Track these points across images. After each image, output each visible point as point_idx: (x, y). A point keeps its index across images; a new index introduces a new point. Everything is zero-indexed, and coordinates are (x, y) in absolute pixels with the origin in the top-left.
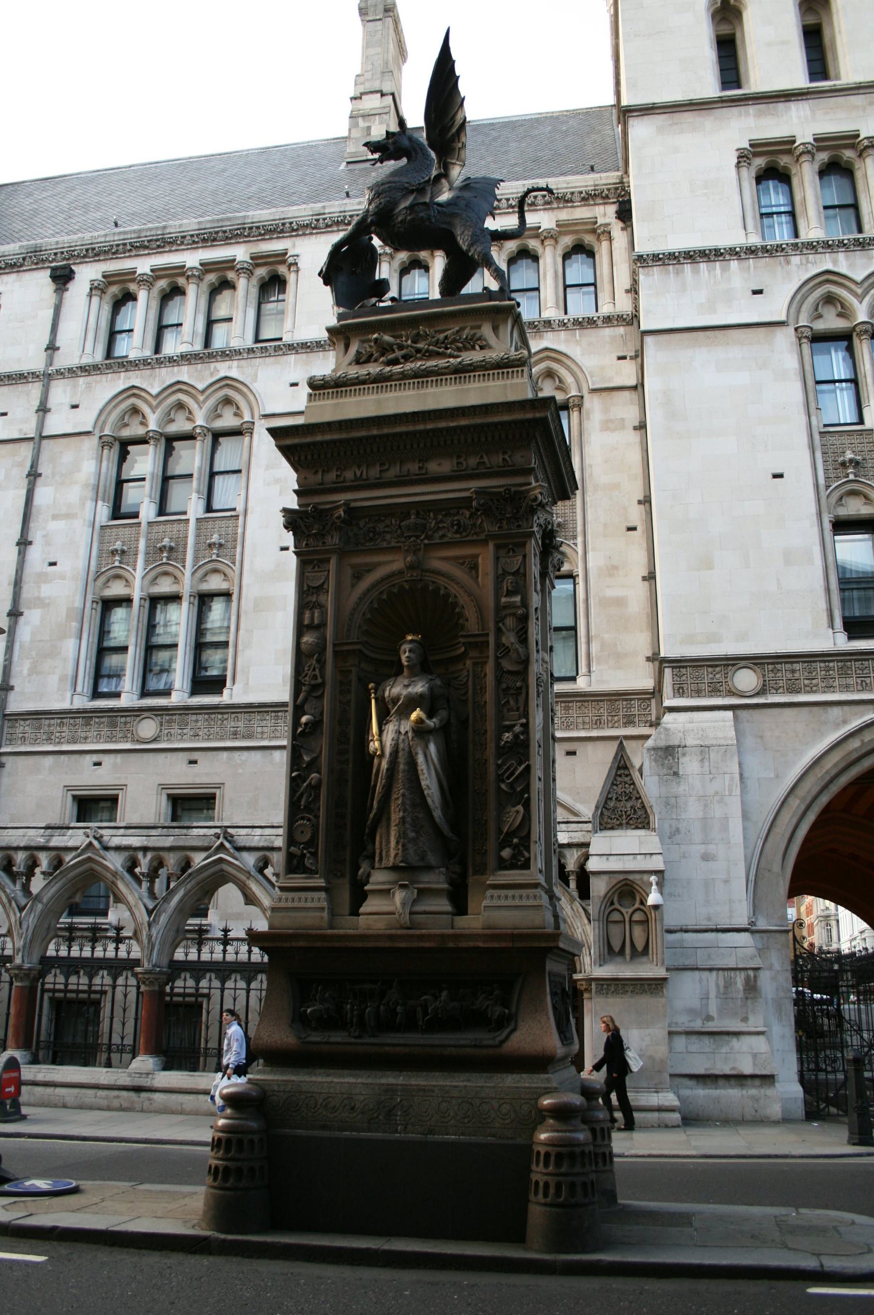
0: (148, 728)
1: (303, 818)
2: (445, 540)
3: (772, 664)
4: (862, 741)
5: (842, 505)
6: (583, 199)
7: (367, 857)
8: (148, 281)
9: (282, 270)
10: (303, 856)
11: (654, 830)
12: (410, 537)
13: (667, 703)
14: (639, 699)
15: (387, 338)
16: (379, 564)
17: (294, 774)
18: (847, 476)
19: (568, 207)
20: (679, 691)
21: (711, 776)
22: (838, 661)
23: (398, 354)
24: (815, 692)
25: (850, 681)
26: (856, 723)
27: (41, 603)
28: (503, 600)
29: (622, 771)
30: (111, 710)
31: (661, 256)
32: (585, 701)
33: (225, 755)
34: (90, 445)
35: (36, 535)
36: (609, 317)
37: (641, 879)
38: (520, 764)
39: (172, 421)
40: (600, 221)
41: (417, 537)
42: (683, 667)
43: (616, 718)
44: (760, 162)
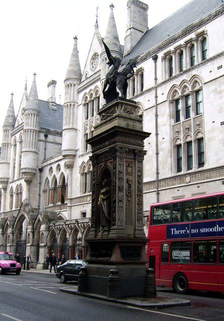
0: (188, 179)
8: (175, 52)
9: (205, 36)
15: (104, 114)
27: (162, 150)
30: (179, 176)
33: (205, 184)
34: (167, 104)
35: (159, 132)
39: (185, 91)
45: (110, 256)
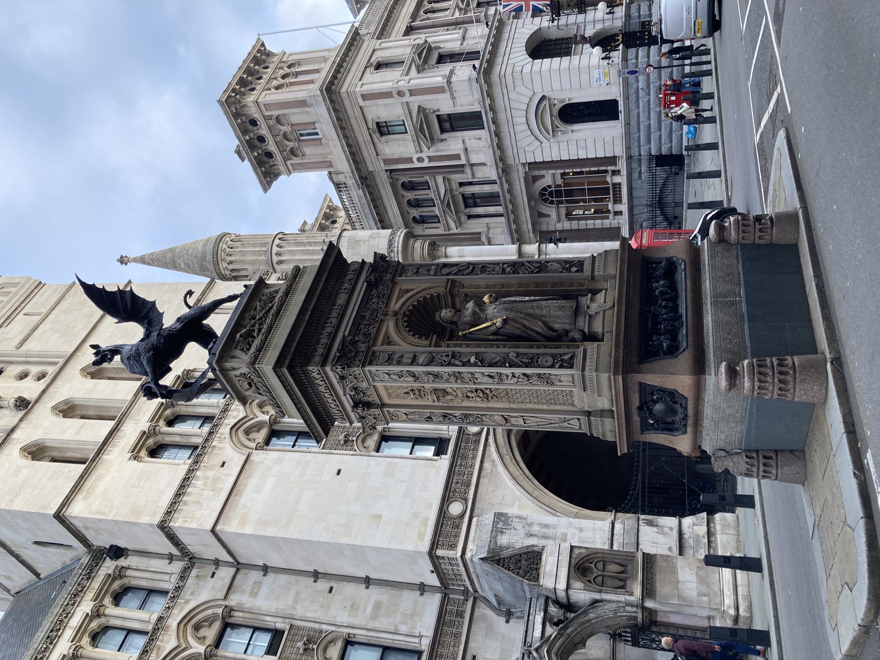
1: (537, 361)
2: (385, 302)
3: (449, 493)
4: (506, 455)
5: (368, 448)
6: (88, 579)
7: (567, 336)
10: (562, 360)
11: (543, 547)
12: (377, 316)
13: (459, 554)
14: (447, 605)
16: (387, 332)
17: (507, 365)
18: (353, 441)
19: (86, 591)
20: (453, 547)
21: (513, 529)
22: (457, 459)
23: (257, 326)
24: (472, 474)
25: (470, 456)
26: (495, 455)
28: (432, 272)
29: (501, 563)
31: (169, 510)
32: (439, 642)
36: (181, 577)
37: (575, 558)
38: (524, 265)
40: (110, 572)
41: (378, 313)
42: (438, 542)
43: (456, 623)
44: (143, 453)
45: (671, 266)
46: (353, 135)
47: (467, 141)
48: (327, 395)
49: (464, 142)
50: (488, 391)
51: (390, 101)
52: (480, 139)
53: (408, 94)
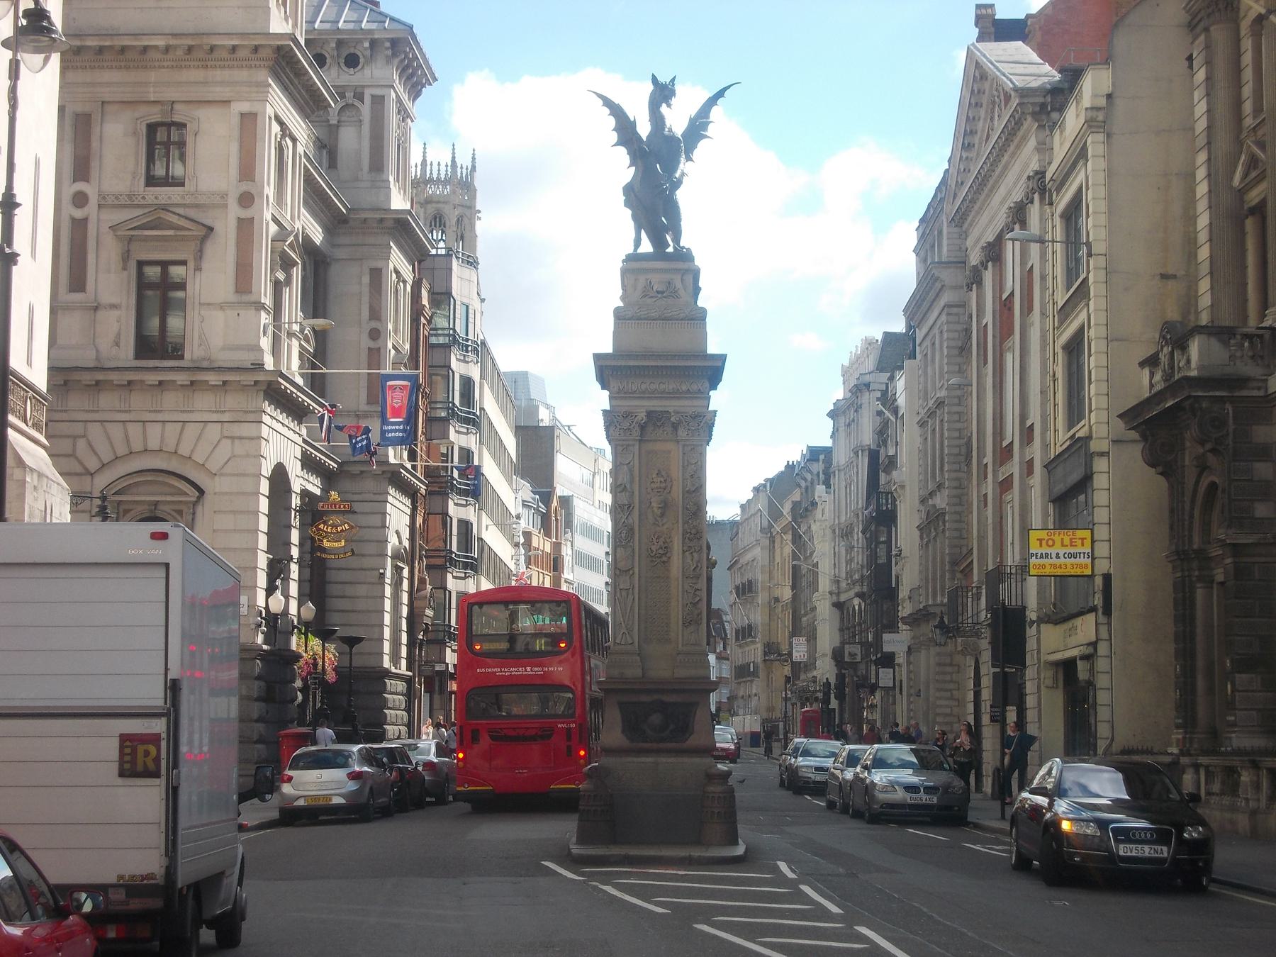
46: (165, 64)
47: (116, 313)
48: (662, 386)
49: (114, 306)
50: (664, 559)
51: (234, 172)
52: (117, 344)
53: (245, 214)
